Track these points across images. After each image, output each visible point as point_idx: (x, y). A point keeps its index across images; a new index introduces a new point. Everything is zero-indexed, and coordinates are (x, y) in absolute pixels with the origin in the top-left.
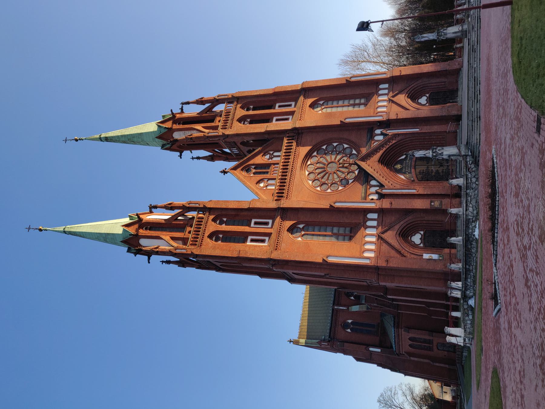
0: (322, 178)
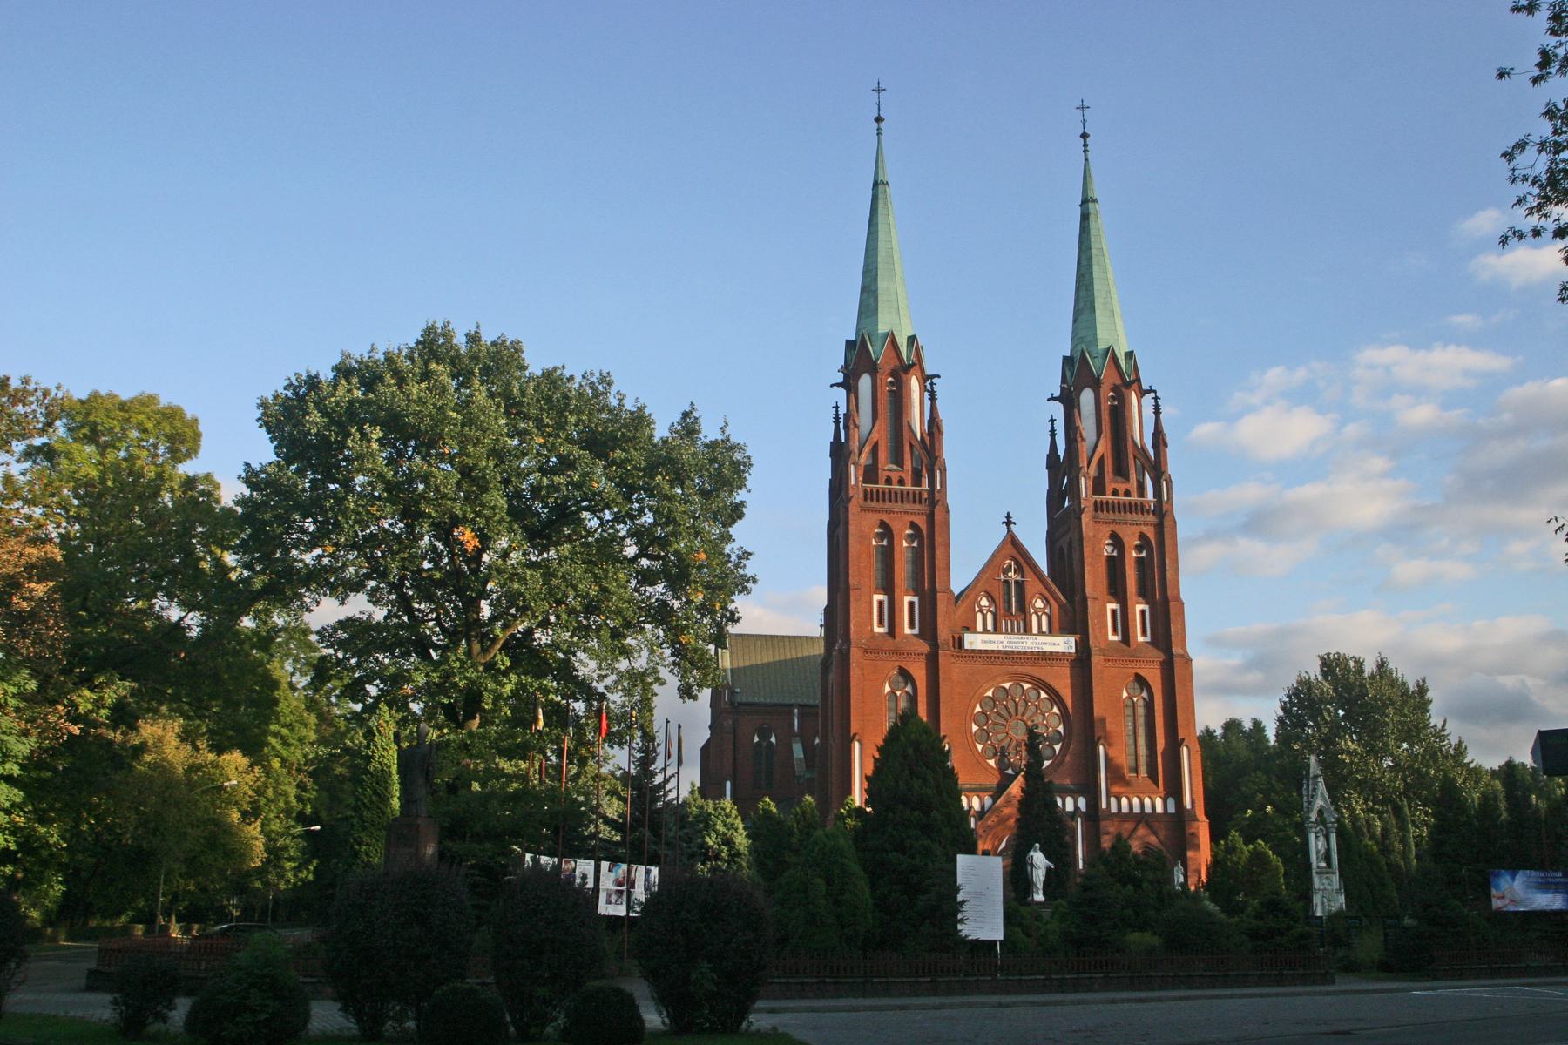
0: (998, 713)
